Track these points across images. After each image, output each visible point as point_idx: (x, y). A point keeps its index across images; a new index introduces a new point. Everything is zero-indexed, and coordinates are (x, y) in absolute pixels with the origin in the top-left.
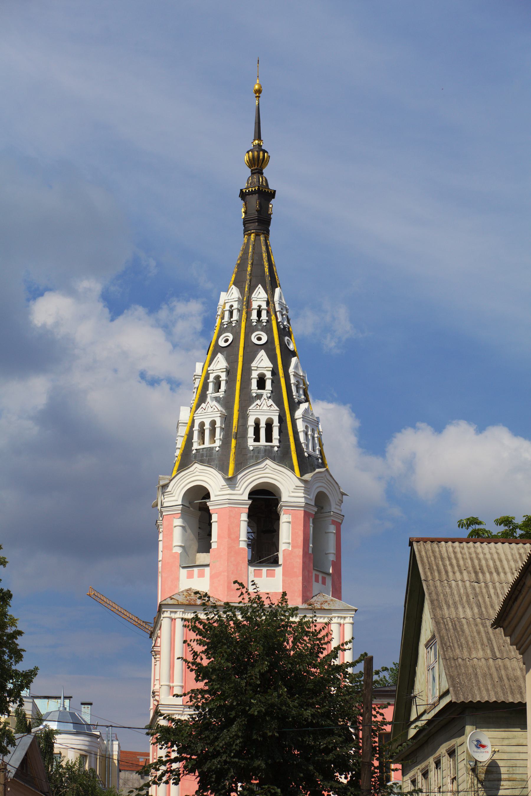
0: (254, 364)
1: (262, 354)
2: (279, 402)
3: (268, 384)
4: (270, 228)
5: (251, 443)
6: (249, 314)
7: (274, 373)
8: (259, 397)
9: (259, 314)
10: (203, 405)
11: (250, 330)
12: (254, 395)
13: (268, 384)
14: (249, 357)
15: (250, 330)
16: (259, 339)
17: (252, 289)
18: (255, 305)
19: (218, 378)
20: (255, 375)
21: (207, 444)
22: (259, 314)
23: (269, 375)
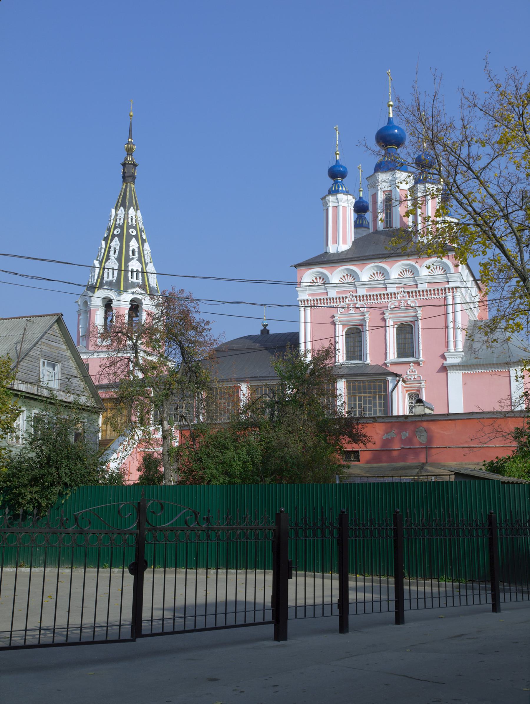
0: (130, 244)
1: (134, 239)
2: (141, 263)
3: (136, 253)
4: (135, 181)
5: (131, 280)
6: (128, 221)
7: (139, 248)
8: (133, 259)
9: (132, 220)
10: (109, 261)
11: (129, 227)
12: (131, 258)
13: (136, 253)
14: (128, 241)
15: (129, 227)
16: (132, 232)
17: (129, 209)
18: (130, 216)
19: (115, 249)
20: (131, 249)
21: (110, 278)
22: (132, 220)
23: (136, 250)
